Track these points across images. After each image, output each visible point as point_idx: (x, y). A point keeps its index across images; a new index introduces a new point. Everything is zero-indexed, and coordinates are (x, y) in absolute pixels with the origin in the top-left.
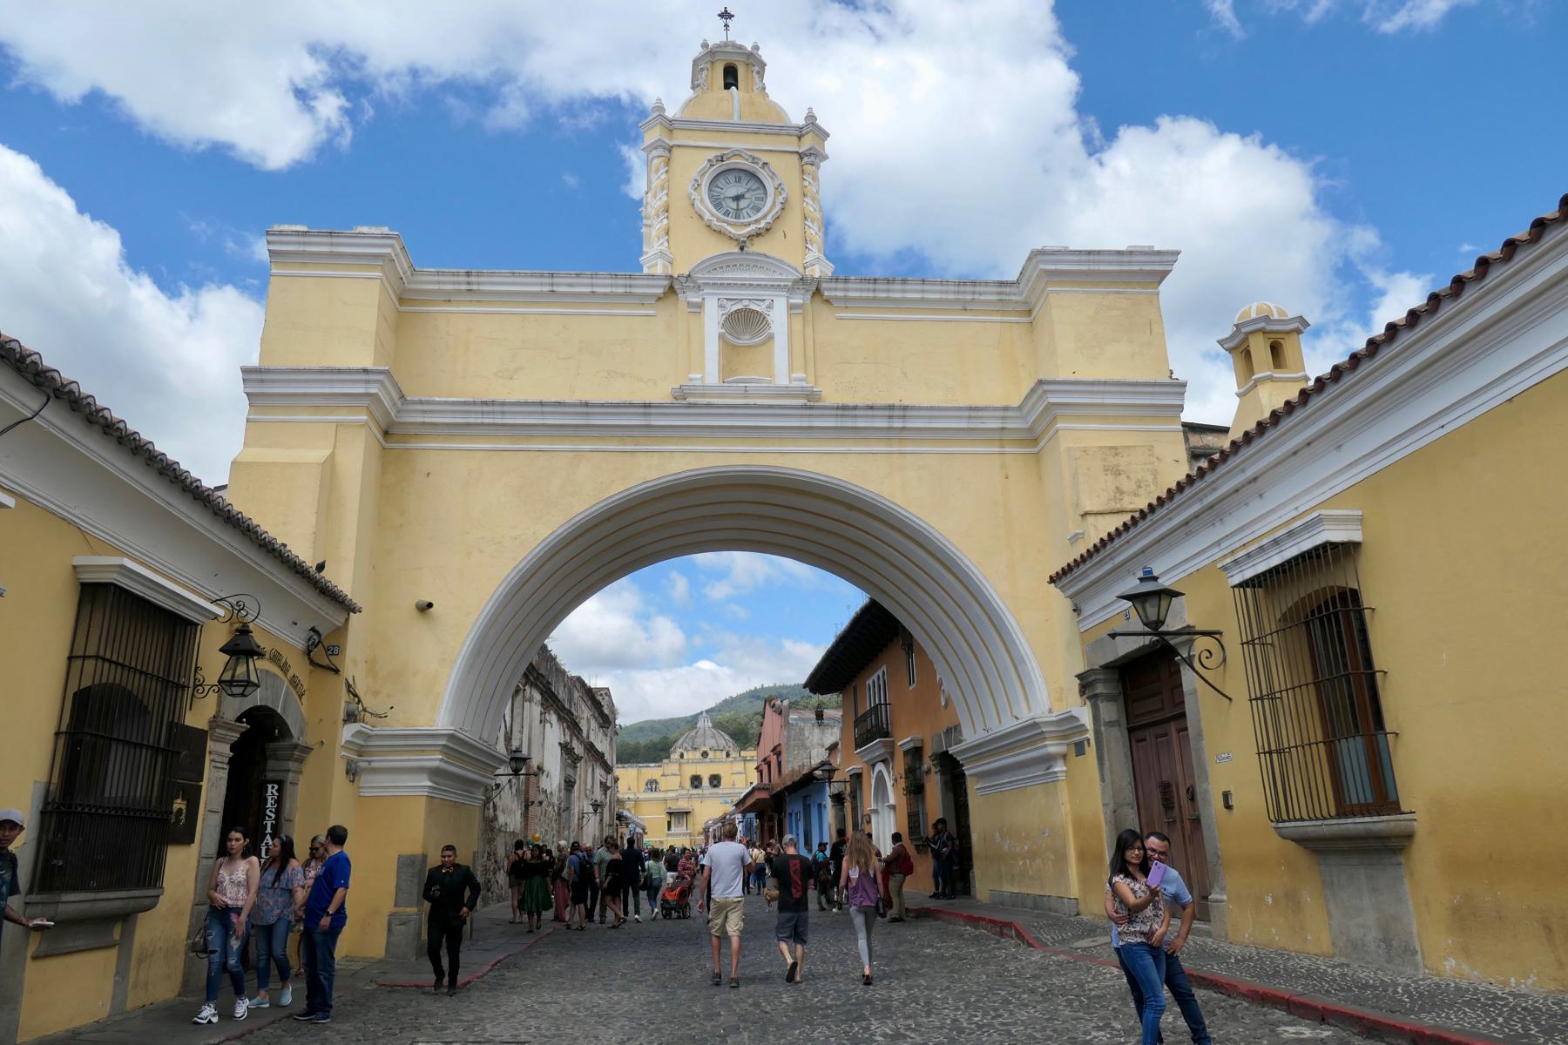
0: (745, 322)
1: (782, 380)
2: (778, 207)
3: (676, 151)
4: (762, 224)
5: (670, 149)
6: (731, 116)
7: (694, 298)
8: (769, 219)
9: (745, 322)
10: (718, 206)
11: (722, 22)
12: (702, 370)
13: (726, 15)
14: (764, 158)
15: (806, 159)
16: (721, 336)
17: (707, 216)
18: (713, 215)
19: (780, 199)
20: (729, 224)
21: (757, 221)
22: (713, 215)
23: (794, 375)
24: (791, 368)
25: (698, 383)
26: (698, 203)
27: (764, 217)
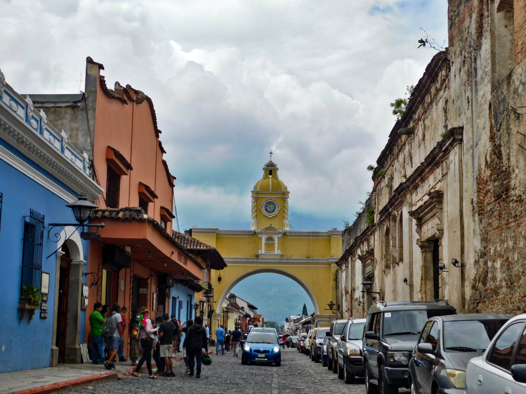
0: (270, 239)
1: (276, 253)
2: (278, 211)
3: (259, 198)
4: (274, 215)
5: (257, 197)
6: (269, 190)
7: (260, 236)
8: (276, 214)
9: (270, 239)
10: (266, 210)
11: (270, 155)
12: (261, 250)
14: (275, 199)
15: (285, 199)
16: (265, 243)
17: (264, 214)
18: (265, 213)
19: (279, 209)
20: (268, 215)
21: (274, 214)
22: (265, 213)
23: (278, 251)
24: (278, 249)
25: (261, 253)
26: (262, 211)
27: (275, 213)
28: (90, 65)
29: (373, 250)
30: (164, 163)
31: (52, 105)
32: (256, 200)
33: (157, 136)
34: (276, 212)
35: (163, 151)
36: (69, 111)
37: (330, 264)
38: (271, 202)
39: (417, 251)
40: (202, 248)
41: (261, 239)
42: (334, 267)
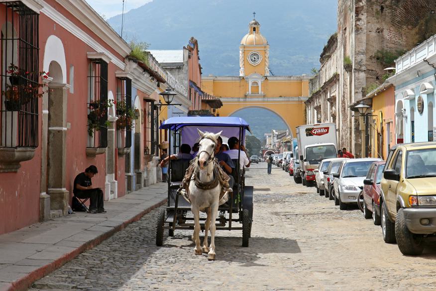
12: (248, 91)
13: (254, 13)
28: (185, 50)
29: (320, 106)
30: (199, 66)
31: (169, 67)
32: (244, 52)
33: (198, 54)
34: (259, 61)
35: (199, 59)
36: (177, 70)
37: (302, 102)
38: (255, 54)
39: (332, 118)
40: (210, 99)
41: (247, 82)
42: (304, 105)
